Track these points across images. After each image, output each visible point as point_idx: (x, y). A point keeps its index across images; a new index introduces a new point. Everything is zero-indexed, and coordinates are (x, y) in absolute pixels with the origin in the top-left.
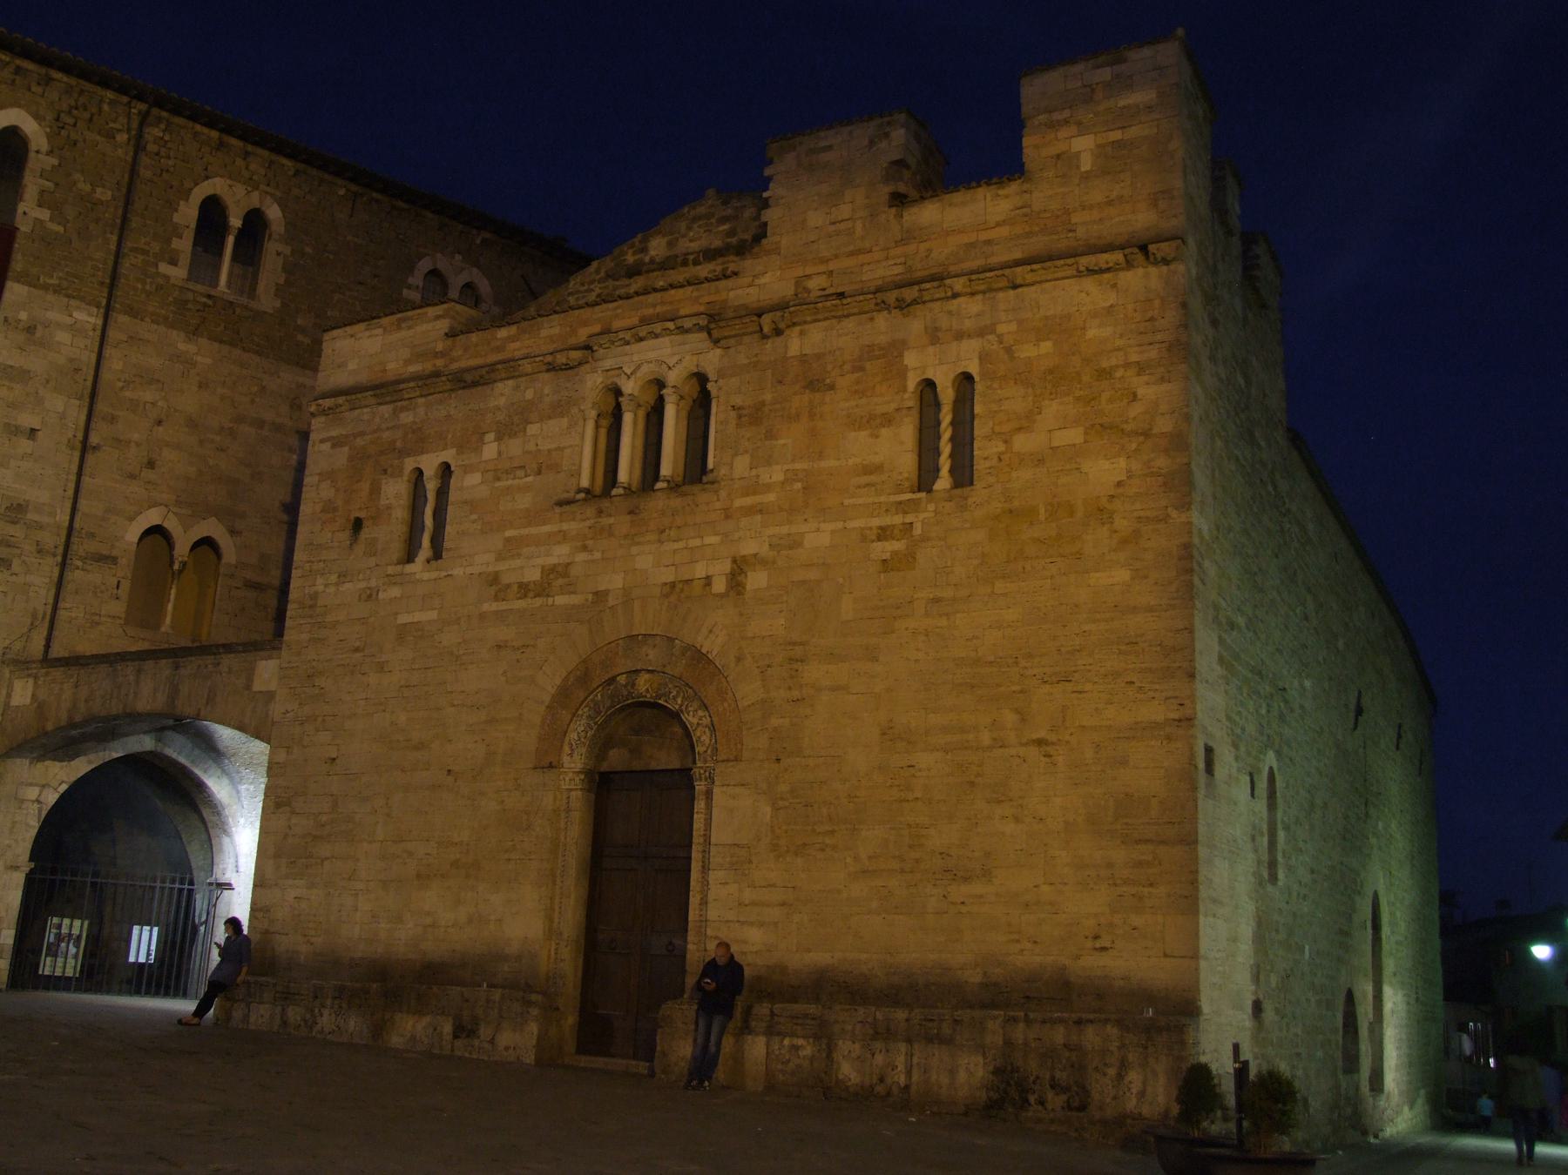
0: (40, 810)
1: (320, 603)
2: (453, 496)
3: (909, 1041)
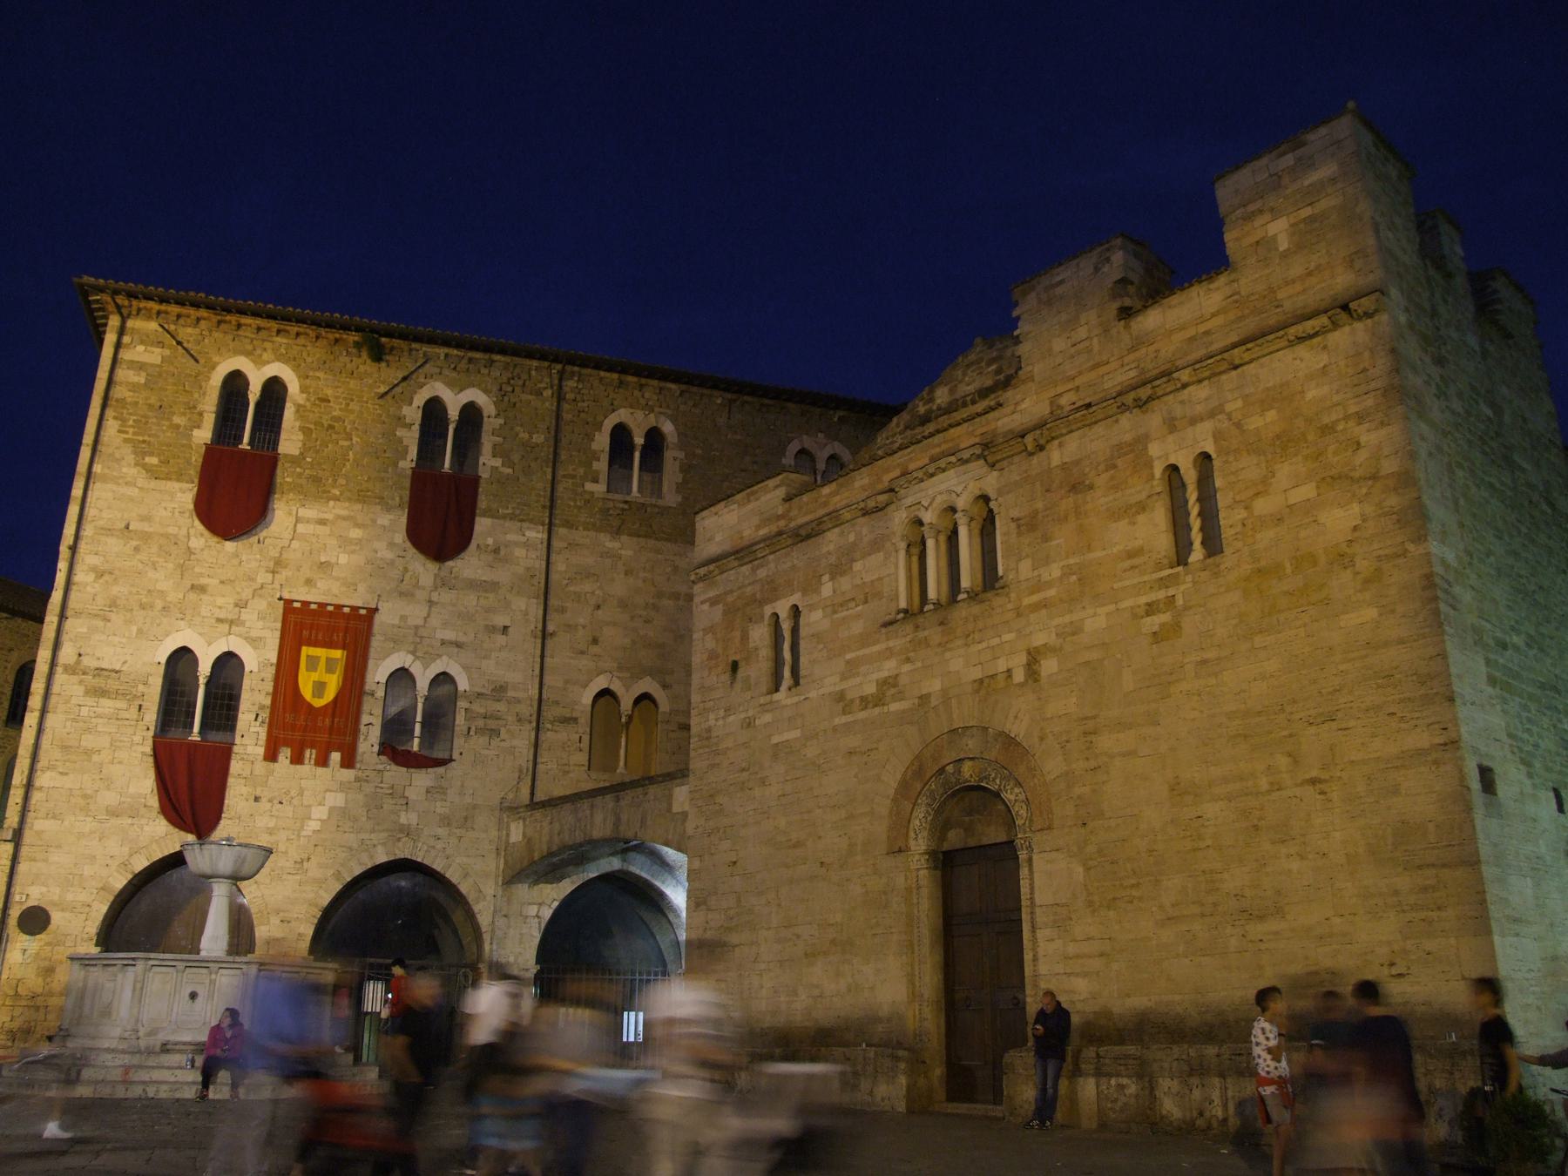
0: (540, 923)
1: (714, 734)
2: (803, 632)
3: (1222, 1075)
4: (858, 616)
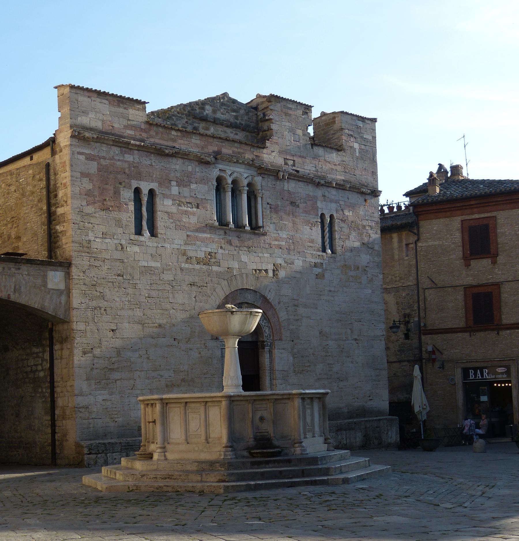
1: (94, 245)
4: (194, 214)
